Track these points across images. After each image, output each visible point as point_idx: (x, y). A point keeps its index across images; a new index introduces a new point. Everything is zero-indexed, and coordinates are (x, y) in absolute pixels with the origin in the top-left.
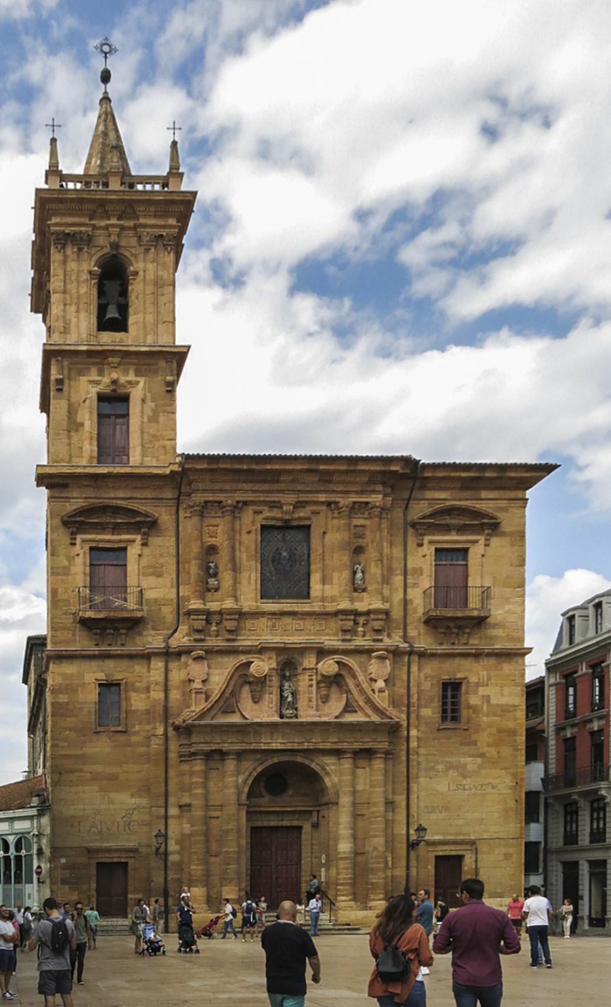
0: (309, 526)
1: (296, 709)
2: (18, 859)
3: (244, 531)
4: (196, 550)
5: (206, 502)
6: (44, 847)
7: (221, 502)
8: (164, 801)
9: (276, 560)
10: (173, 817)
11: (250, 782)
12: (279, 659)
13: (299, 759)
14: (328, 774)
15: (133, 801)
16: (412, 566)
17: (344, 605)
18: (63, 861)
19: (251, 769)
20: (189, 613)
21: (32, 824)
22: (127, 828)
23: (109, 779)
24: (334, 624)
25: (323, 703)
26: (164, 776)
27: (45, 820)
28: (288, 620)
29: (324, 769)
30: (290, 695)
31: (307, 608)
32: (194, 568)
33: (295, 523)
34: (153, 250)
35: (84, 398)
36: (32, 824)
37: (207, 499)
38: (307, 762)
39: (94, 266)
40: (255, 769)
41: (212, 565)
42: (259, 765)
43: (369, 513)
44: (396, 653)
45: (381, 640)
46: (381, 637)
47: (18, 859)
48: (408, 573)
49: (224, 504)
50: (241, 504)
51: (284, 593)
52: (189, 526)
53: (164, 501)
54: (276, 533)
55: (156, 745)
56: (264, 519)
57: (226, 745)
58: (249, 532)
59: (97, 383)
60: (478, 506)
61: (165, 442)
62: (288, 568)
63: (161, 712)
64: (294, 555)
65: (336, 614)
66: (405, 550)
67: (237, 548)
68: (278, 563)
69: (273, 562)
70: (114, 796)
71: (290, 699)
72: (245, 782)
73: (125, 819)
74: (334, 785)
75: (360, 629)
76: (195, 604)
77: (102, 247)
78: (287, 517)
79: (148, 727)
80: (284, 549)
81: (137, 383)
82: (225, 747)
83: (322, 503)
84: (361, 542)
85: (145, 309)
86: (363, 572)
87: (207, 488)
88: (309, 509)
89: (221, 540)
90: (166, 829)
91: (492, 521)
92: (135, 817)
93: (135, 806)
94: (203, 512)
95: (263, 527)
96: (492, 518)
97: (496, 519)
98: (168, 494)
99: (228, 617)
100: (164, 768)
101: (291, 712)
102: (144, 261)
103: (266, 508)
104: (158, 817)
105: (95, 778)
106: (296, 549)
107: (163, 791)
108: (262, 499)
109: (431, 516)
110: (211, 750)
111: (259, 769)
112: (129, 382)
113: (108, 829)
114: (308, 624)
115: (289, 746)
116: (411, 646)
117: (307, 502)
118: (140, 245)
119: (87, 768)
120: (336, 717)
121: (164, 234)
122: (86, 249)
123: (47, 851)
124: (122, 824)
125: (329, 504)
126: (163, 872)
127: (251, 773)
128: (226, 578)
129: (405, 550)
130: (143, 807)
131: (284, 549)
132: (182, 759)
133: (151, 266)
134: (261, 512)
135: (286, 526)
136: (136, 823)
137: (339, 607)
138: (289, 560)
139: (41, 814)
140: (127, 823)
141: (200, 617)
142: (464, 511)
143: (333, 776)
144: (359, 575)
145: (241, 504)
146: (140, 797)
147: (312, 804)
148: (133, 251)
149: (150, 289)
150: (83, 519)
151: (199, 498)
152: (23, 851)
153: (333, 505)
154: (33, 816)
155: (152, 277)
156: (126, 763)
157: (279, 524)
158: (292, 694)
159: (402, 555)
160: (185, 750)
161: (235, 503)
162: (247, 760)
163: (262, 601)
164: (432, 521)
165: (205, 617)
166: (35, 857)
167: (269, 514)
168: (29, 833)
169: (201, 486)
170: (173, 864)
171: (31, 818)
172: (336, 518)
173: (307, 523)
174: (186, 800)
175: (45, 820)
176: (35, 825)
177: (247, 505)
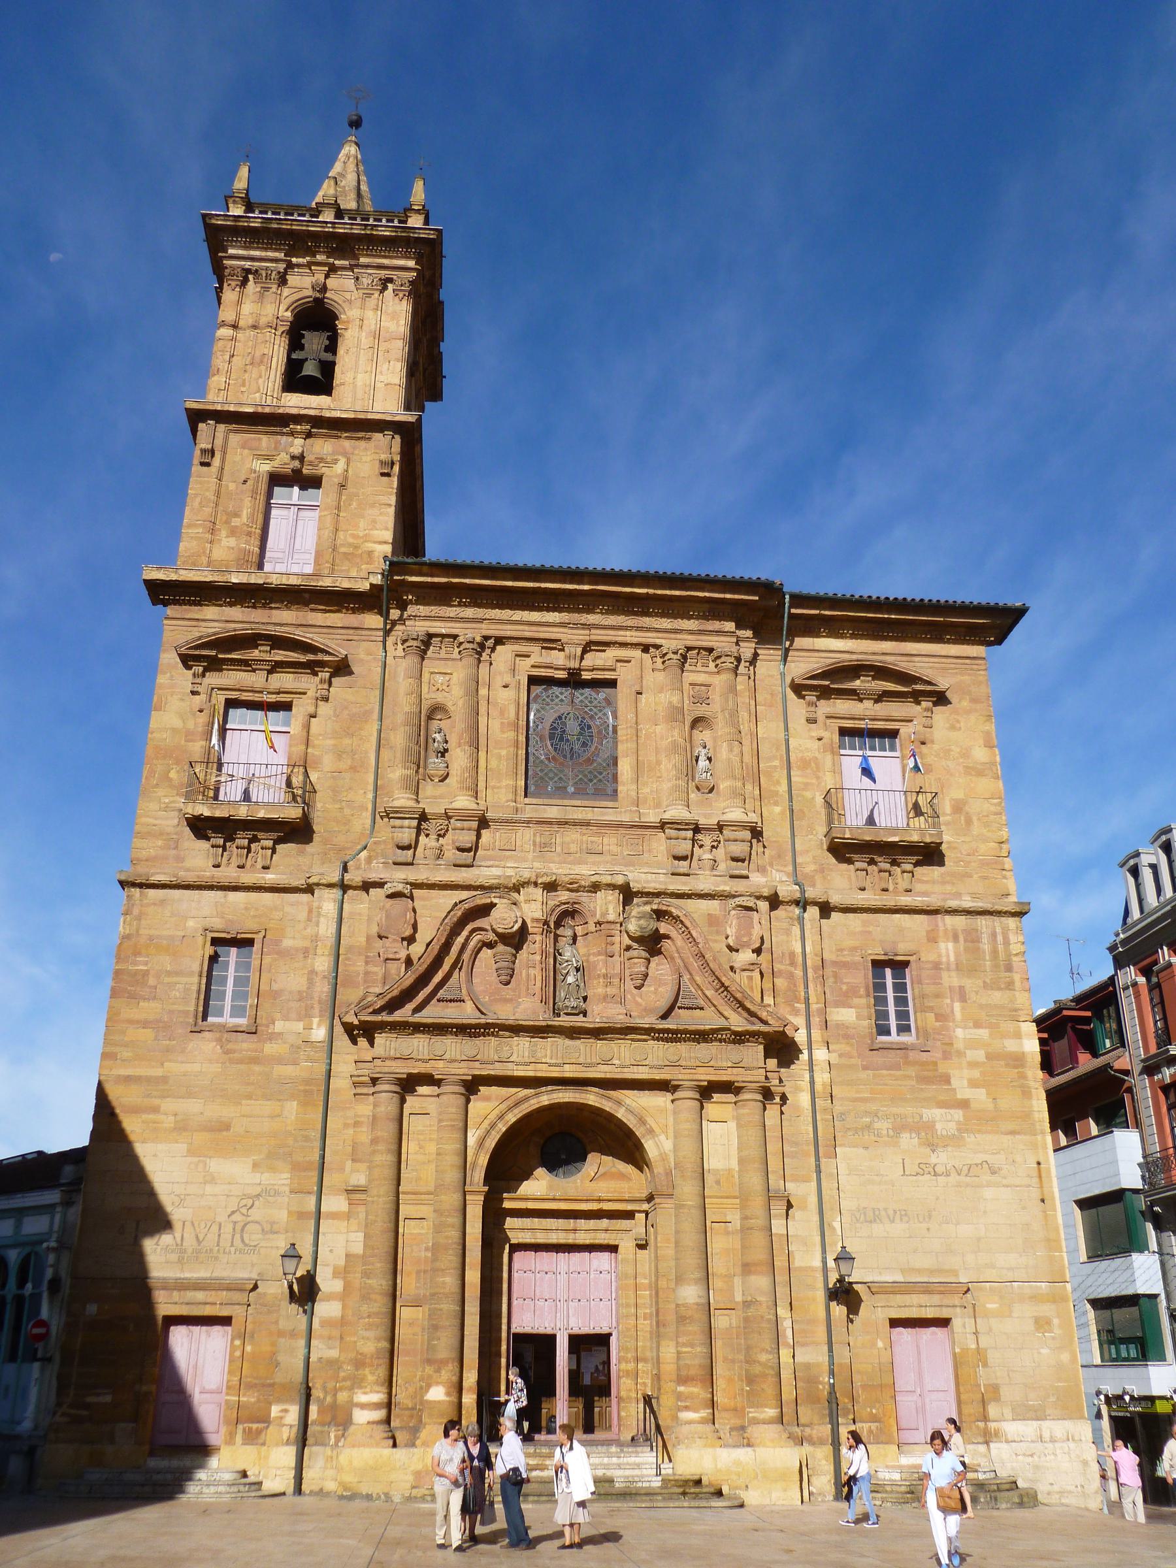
0: (612, 684)
1: (585, 999)
2: (19, 1300)
3: (498, 682)
4: (407, 709)
5: (430, 636)
6: (63, 1274)
7: (457, 636)
8: (315, 1179)
9: (557, 734)
10: (334, 1216)
11: (491, 1143)
12: (551, 903)
13: (592, 1098)
14: (651, 1131)
15: (257, 1178)
16: (800, 755)
17: (676, 812)
18: (92, 1309)
19: (493, 1117)
20: (387, 815)
21: (52, 1223)
22: (238, 1236)
23: (213, 1130)
24: (660, 845)
25: (638, 988)
26: (319, 1126)
27: (74, 1212)
28: (572, 836)
29: (642, 1121)
30: (573, 972)
31: (610, 816)
32: (399, 739)
33: (586, 676)
34: (377, 294)
35: (243, 478)
36: (52, 1223)
37: (432, 631)
38: (607, 1106)
39: (287, 310)
40: (501, 1117)
41: (437, 735)
42: (510, 1109)
43: (716, 666)
44: (774, 902)
45: (747, 877)
46: (744, 872)
47: (19, 1300)
48: (793, 765)
49: (461, 639)
50: (492, 641)
51: (571, 789)
52: (401, 664)
53: (364, 632)
54: (556, 690)
55: (310, 1067)
56: (533, 666)
57: (441, 1064)
58: (505, 687)
59: (269, 458)
60: (903, 664)
61: (370, 545)
62: (577, 747)
63: (324, 996)
64: (589, 727)
65: (663, 825)
66: (787, 729)
67: (483, 709)
68: (561, 739)
69: (552, 737)
70: (217, 1165)
71: (570, 979)
72: (481, 1143)
73: (237, 1217)
74: (663, 1157)
75: (707, 856)
76: (402, 800)
77: (301, 289)
78: (574, 664)
79: (299, 1026)
80: (571, 715)
81: (336, 461)
82: (437, 1068)
83: (634, 645)
84: (701, 711)
85: (357, 366)
86: (710, 759)
87: (433, 614)
88: (612, 653)
89: (455, 698)
90: (316, 1244)
91: (929, 688)
92: (255, 1214)
93: (258, 1190)
94: (425, 652)
95: (533, 681)
96: (929, 683)
97: (935, 685)
98: (373, 620)
99: (459, 824)
100: (321, 1109)
101: (574, 1004)
102: (363, 308)
103: (535, 649)
104: (301, 1215)
105: (182, 1127)
106: (592, 717)
107: (316, 1157)
108: (528, 634)
109: (824, 675)
110: (409, 1075)
111: (512, 1118)
112: (321, 460)
113: (197, 1237)
114: (610, 841)
115: (569, 1072)
116: (803, 892)
117: (608, 644)
118: (357, 289)
119: (168, 1105)
120: (664, 1017)
121: (395, 277)
122: (274, 290)
123: (66, 1282)
124: (228, 1229)
125: (646, 648)
126: (302, 1342)
127: (493, 1126)
128: (459, 758)
129: (787, 729)
130: (277, 1193)
131: (571, 715)
132: (359, 1090)
133: (370, 314)
134: (528, 656)
135: (574, 680)
136: (257, 1227)
137: (667, 816)
138: (580, 734)
139: (67, 1203)
140: (238, 1228)
141: (406, 822)
142: (881, 672)
143: (662, 1137)
144: (703, 763)
145: (490, 643)
146: (273, 1169)
147: (616, 1196)
148: (347, 296)
149: (366, 341)
150: (213, 653)
151: (420, 627)
152: (29, 1286)
153: (652, 650)
154: (52, 1206)
155: (373, 327)
156: (249, 1097)
157: (562, 675)
158: (578, 970)
159: (782, 735)
160: (366, 1072)
161: (478, 639)
162: (487, 1099)
163: (527, 800)
164: (827, 683)
165: (415, 823)
166: (45, 1295)
167: (541, 660)
168: (41, 1242)
169: (422, 610)
170: (326, 1323)
171: (49, 1208)
172: (659, 670)
173: (608, 675)
174: (360, 1179)
175: (74, 1212)
176: (56, 1227)
177: (504, 644)
